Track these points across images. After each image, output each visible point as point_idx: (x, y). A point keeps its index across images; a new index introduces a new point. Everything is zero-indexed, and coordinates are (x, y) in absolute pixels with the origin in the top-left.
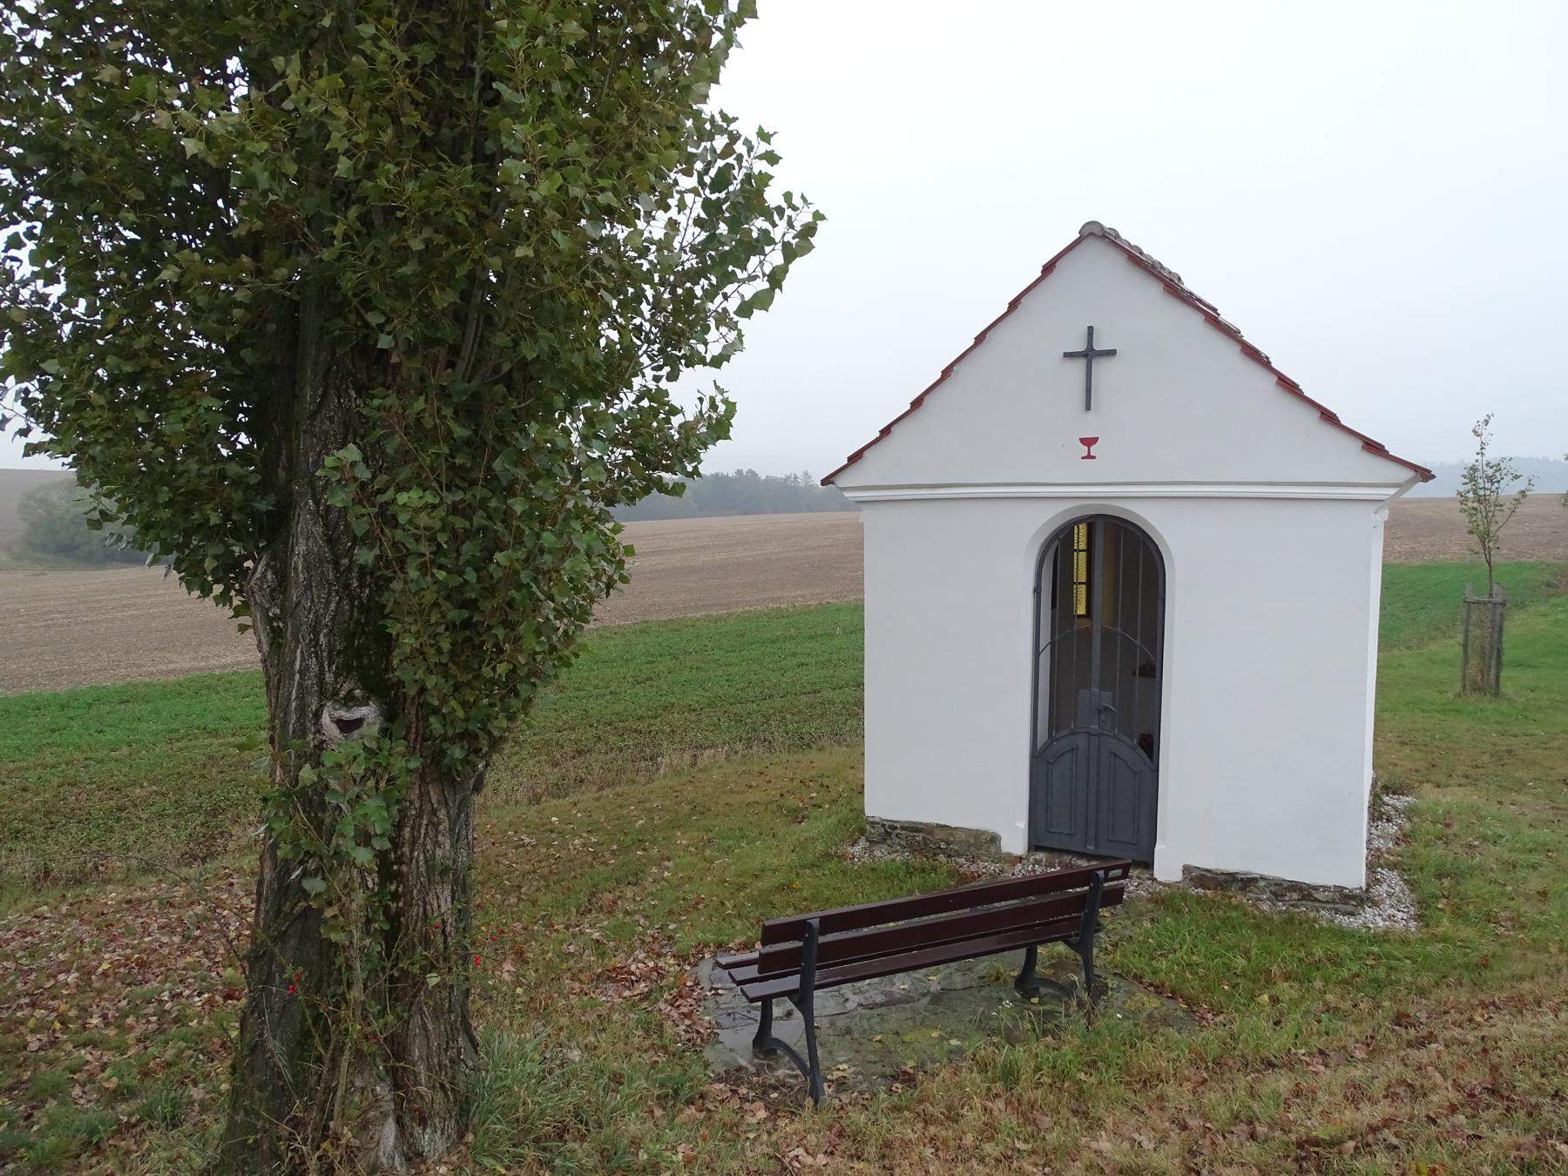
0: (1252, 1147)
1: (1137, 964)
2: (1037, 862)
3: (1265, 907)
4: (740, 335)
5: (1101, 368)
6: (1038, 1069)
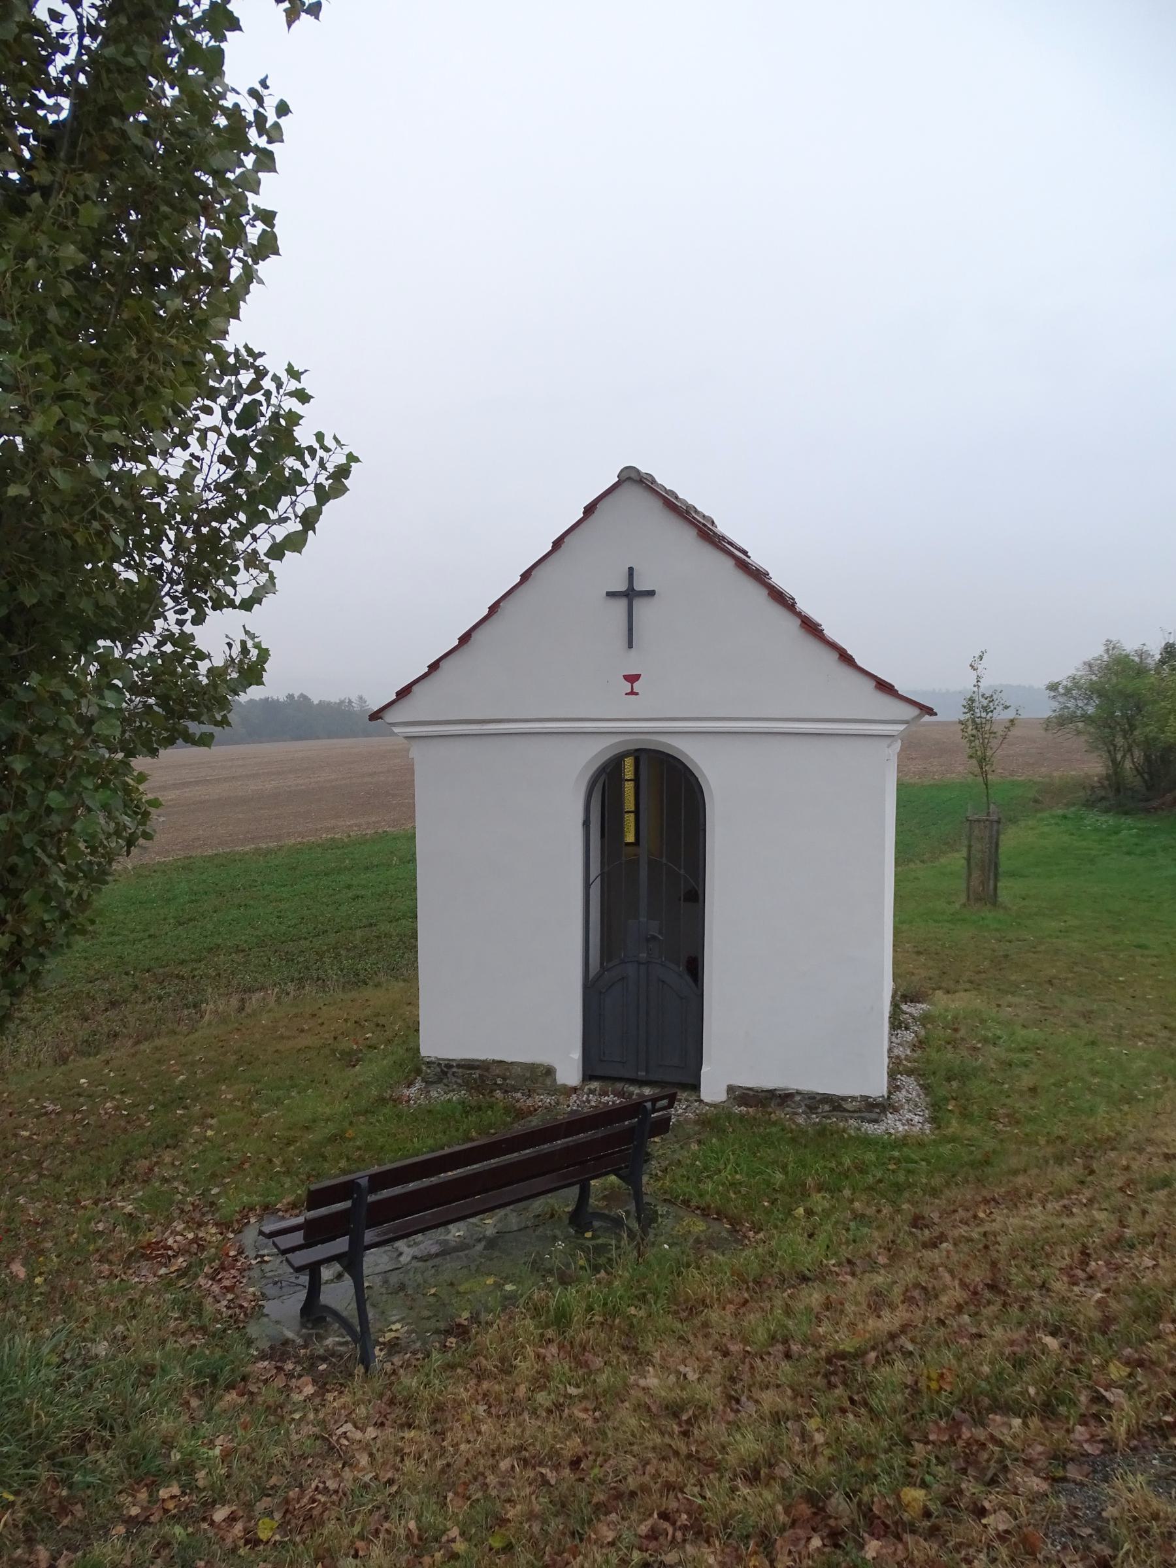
0: (786, 1366)
1: (684, 1188)
2: (591, 1092)
3: (801, 1120)
4: (272, 578)
5: (640, 605)
6: (590, 1309)
